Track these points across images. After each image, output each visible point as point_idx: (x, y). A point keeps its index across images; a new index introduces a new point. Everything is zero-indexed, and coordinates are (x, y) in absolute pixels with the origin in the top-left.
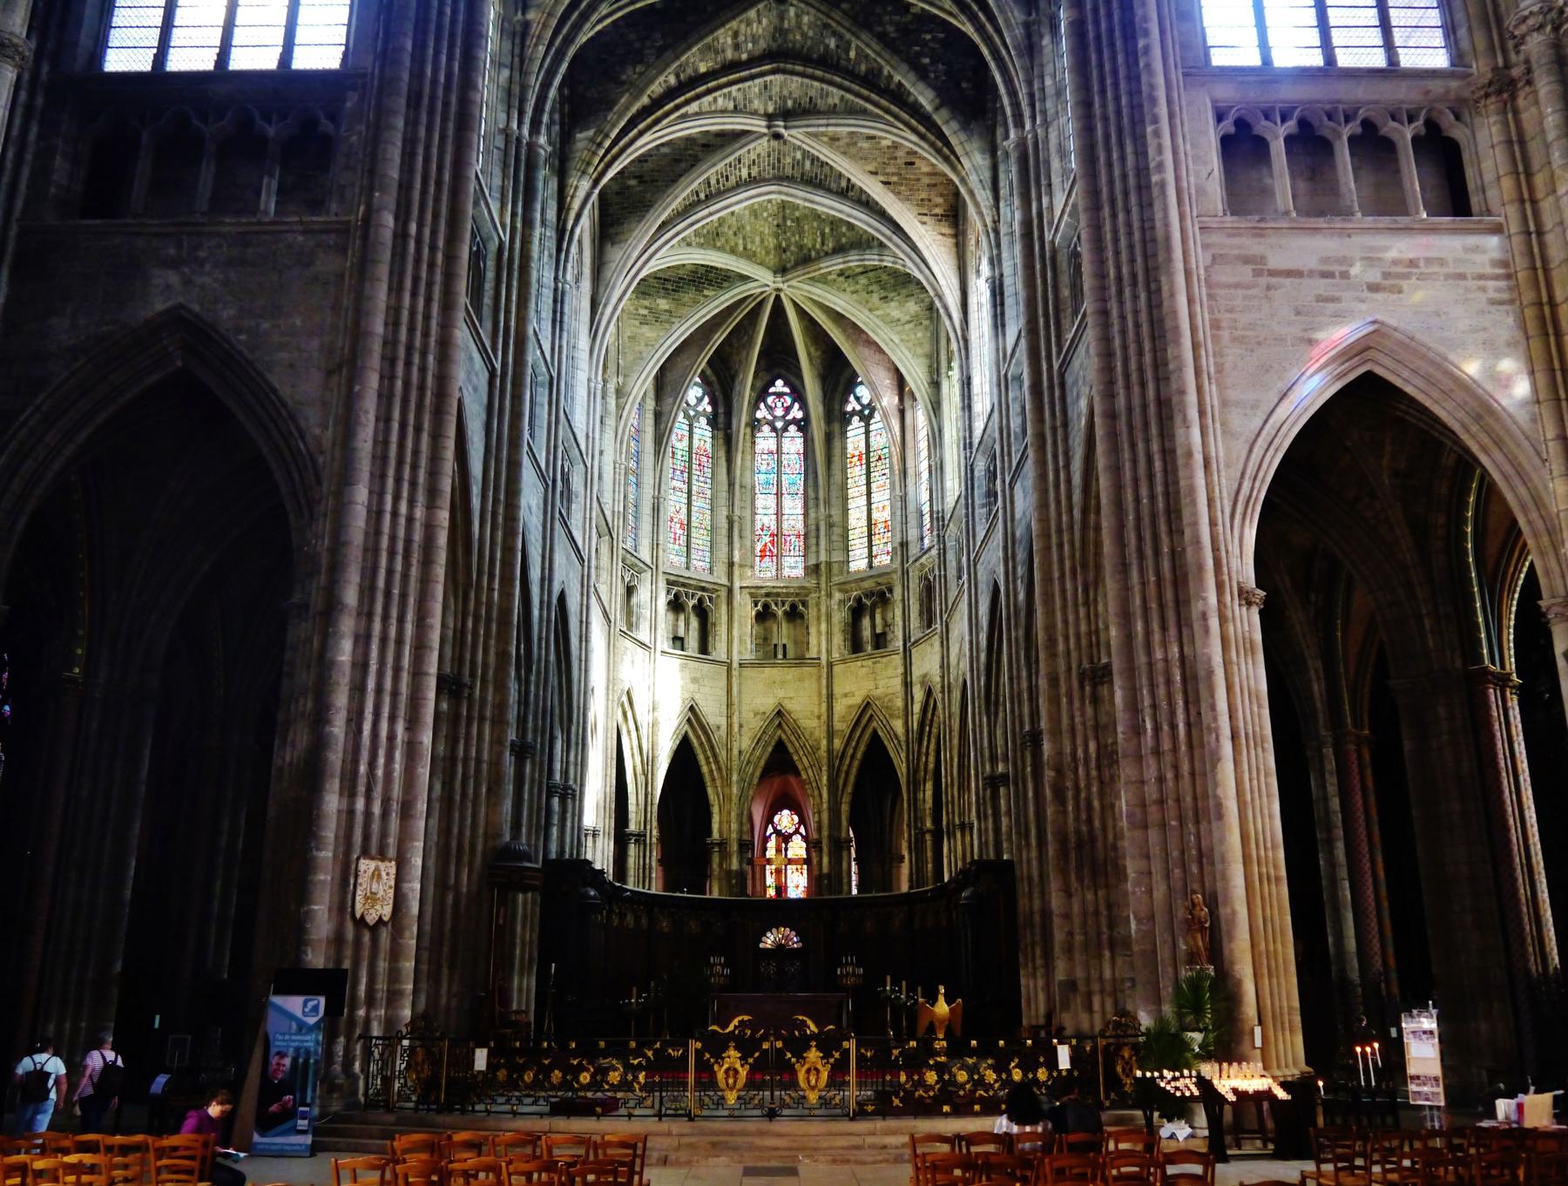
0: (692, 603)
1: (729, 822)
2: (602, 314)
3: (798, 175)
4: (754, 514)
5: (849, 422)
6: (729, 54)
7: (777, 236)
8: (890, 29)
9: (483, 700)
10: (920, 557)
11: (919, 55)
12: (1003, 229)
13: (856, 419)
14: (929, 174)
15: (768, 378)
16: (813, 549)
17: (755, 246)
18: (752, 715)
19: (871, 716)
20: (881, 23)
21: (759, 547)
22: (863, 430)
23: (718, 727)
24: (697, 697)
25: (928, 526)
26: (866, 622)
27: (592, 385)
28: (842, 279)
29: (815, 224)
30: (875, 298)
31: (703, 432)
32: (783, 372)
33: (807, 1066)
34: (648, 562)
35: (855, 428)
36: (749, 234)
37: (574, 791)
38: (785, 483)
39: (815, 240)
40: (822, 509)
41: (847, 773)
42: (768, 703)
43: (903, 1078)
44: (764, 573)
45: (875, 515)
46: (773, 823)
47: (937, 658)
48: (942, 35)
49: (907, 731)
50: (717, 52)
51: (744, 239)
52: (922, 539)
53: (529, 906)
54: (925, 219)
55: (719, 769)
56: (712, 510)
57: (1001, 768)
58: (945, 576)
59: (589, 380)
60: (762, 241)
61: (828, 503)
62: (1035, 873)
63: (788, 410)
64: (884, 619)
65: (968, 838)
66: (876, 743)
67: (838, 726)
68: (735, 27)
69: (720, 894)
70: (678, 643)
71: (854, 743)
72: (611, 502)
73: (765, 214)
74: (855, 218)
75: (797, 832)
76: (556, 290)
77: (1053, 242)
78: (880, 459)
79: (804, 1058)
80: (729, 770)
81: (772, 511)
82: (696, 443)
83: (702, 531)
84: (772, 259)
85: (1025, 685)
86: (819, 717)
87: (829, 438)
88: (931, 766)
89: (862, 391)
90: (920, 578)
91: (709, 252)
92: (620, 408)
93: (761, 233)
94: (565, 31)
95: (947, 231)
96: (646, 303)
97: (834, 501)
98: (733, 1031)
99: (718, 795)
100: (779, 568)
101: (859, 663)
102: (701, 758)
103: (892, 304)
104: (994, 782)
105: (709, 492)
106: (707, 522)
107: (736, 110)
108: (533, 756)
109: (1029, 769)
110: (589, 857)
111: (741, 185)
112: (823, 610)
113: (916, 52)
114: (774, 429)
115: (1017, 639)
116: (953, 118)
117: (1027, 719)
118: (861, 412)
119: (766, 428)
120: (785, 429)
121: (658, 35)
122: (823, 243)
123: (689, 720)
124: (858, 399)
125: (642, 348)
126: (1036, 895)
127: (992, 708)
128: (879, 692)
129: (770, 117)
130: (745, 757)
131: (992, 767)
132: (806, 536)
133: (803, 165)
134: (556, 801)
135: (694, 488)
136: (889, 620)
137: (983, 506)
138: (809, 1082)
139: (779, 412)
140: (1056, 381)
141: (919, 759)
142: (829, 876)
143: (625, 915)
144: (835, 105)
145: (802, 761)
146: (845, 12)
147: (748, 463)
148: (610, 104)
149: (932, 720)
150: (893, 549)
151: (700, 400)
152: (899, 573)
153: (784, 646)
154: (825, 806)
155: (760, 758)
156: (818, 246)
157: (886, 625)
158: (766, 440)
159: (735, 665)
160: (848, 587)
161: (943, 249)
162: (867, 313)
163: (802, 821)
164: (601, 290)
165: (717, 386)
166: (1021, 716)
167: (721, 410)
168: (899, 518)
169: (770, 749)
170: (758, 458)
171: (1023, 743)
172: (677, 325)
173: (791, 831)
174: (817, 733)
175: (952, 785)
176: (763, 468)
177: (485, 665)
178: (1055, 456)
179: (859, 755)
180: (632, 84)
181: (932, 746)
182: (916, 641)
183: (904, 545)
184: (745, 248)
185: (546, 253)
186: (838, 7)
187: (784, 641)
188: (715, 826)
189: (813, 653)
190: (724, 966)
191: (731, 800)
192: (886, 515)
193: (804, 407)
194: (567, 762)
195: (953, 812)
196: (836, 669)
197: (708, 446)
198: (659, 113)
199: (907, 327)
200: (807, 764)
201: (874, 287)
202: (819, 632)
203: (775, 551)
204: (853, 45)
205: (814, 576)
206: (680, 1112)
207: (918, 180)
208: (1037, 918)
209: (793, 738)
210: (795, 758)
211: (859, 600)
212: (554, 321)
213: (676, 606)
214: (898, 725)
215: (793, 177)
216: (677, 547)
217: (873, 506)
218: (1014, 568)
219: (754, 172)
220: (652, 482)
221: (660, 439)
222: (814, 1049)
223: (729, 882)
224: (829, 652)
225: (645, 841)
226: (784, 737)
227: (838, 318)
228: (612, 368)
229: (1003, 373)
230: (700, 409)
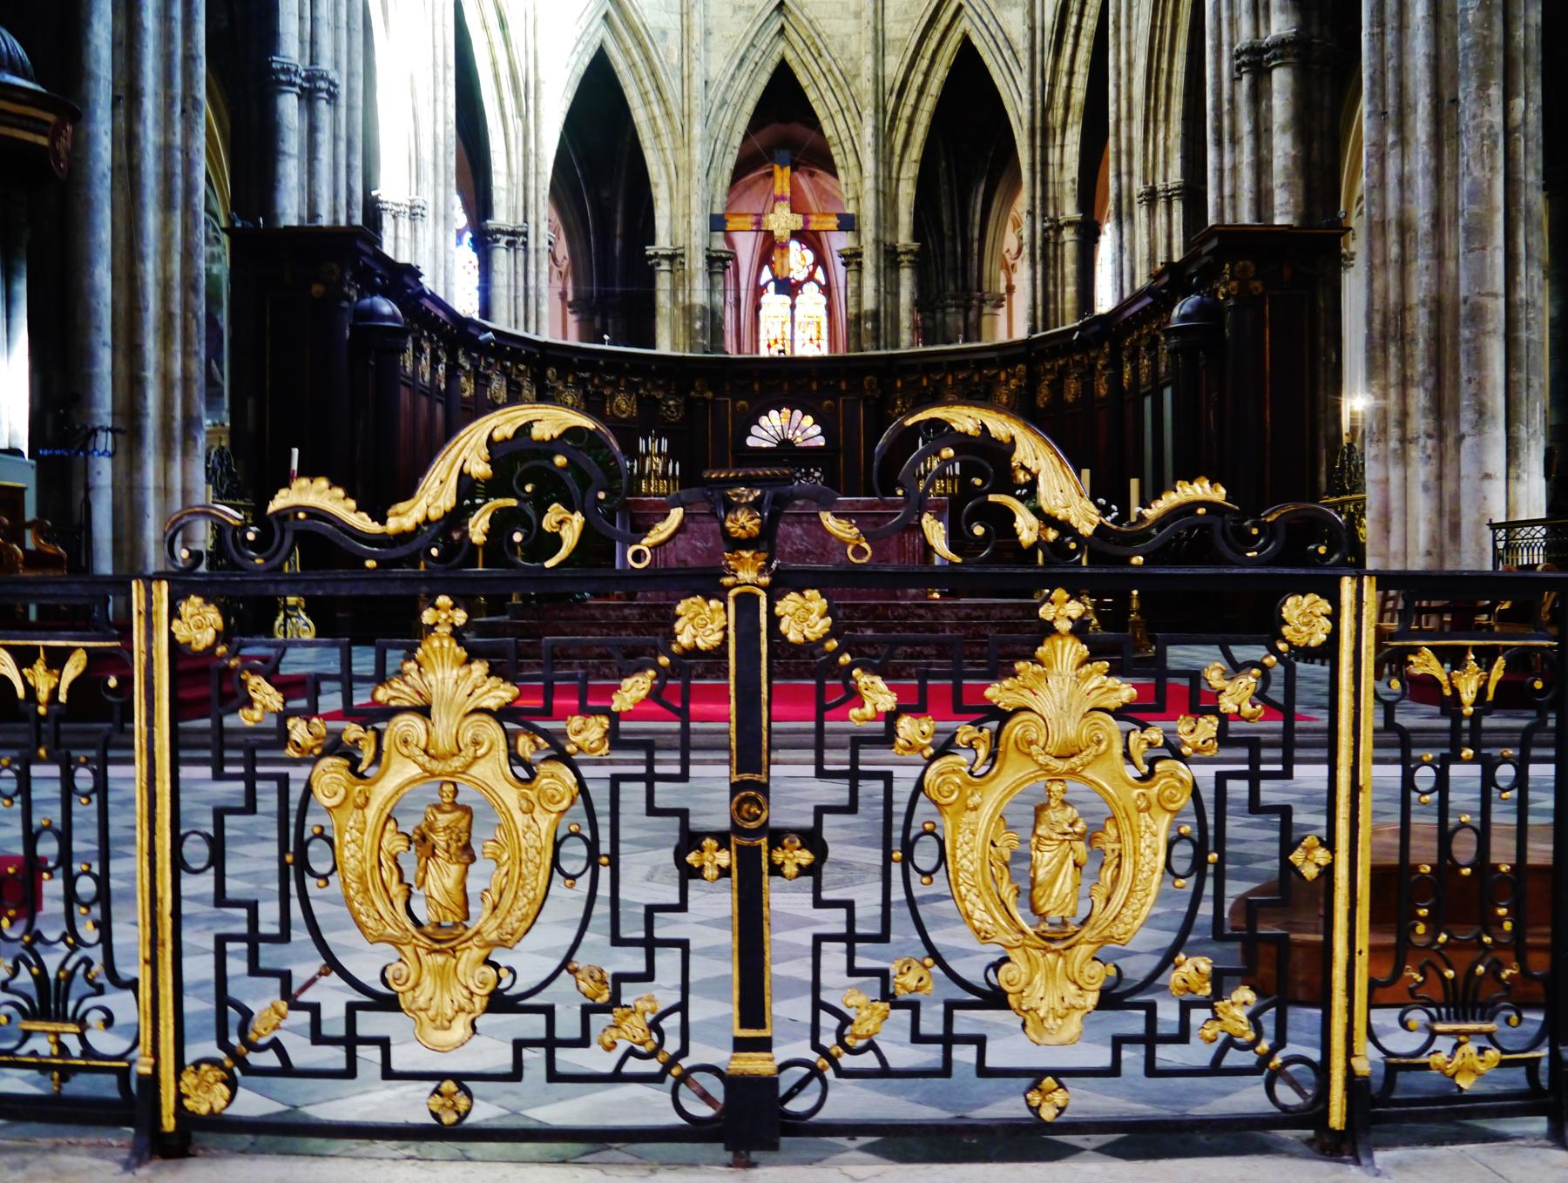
18: (728, 11)
19: (960, 7)
23: (664, 33)
33: (1014, 773)
37: (332, 83)
41: (911, 123)
49: (1032, 29)
53: (177, 296)
55: (668, 114)
65: (1161, 219)
66: (968, 62)
69: (674, 345)
71: (924, 64)
75: (811, 277)
80: (687, 116)
86: (858, 15)
88: (1079, 96)
98: (458, 516)
99: (666, 165)
110: (404, 258)
123: (606, 17)
126: (1421, 262)
130: (715, 94)
134: (289, 106)
138: (1029, 894)
141: (1053, 85)
142: (875, 315)
143: (488, 379)
154: (869, 183)
155: (744, 96)
163: (820, 260)
169: (764, 79)
174: (853, 46)
175: (1130, 117)
179: (935, 87)
181: (1083, 55)
190: (667, 457)
191: (690, 172)
194: (313, 19)
195: (1130, 173)
200: (834, 108)
206: (80, 1086)
208: (1420, 320)
209: (808, 58)
210: (812, 95)
214: (1014, 22)
222: (1066, 652)
223: (689, 328)
225: (525, 244)
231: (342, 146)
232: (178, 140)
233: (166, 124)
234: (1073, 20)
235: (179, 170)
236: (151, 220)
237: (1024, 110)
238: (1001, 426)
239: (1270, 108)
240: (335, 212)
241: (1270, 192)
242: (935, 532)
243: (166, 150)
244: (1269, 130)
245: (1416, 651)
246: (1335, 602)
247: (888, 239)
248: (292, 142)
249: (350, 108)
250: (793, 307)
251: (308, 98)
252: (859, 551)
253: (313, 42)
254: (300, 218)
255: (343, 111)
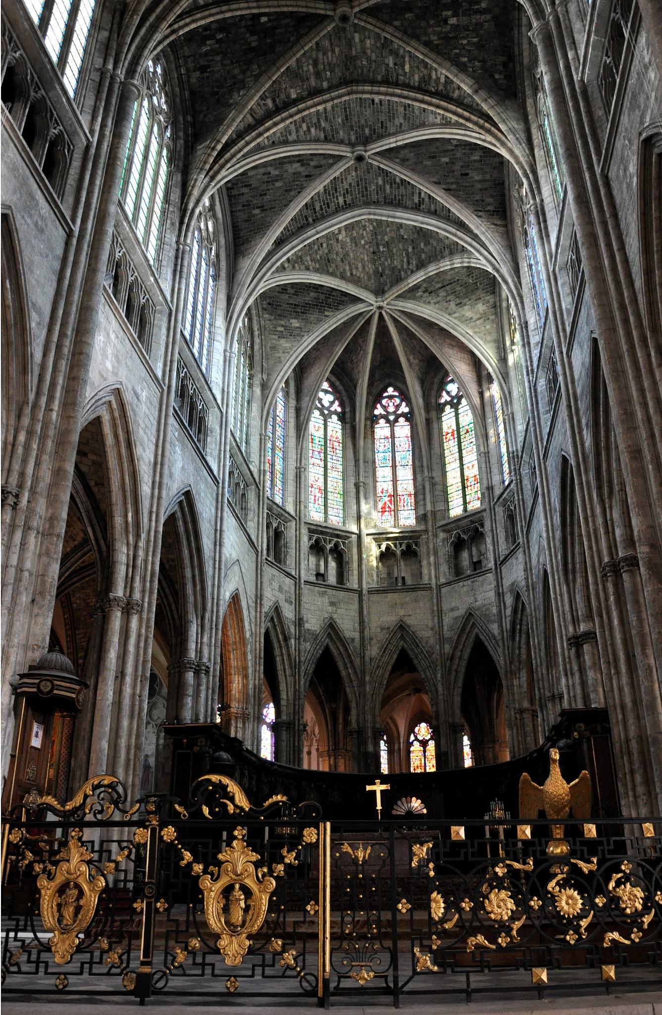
0: (329, 547)
1: (364, 714)
2: (236, 304)
3: (381, 199)
4: (375, 481)
5: (443, 410)
6: (313, 82)
7: (373, 261)
8: (434, 38)
9: (30, 511)
10: (503, 493)
11: (458, 56)
12: (540, 165)
13: (448, 408)
14: (480, 181)
15: (382, 386)
16: (422, 503)
17: (358, 273)
20: (426, 34)
21: (380, 505)
22: (453, 414)
23: (353, 640)
24: (335, 616)
25: (508, 471)
26: (465, 555)
27: (228, 354)
28: (427, 294)
29: (401, 246)
30: (452, 305)
31: (335, 427)
32: (392, 381)
34: (293, 513)
35: (448, 414)
36: (353, 261)
37: (207, 667)
38: (398, 459)
39: (402, 261)
40: (426, 473)
42: (390, 620)
43: (438, 907)
44: (387, 524)
45: (467, 473)
46: (414, 733)
47: (521, 567)
48: (475, 40)
49: (502, 631)
50: (303, 81)
51: (350, 266)
52: (504, 482)
53: (133, 751)
54: (480, 214)
55: (356, 673)
56: (343, 480)
57: (583, 627)
58: (523, 500)
59: (225, 351)
60: (364, 268)
61: (430, 469)
62: (628, 700)
63: (397, 407)
64: (479, 551)
67: (447, 633)
68: (314, 56)
70: (319, 578)
72: (257, 463)
73: (363, 242)
74: (427, 224)
76: (177, 250)
77: (582, 80)
78: (467, 432)
79: (219, 864)
80: (363, 673)
81: (389, 477)
82: (329, 433)
83: (336, 495)
84: (372, 283)
85: (600, 520)
86: (432, 629)
87: (428, 422)
88: (524, 657)
89: (453, 388)
90: (504, 512)
91: (323, 276)
92: (264, 398)
93: (363, 259)
94: (158, 10)
95: (499, 223)
96: (282, 322)
97: (435, 467)
100: (396, 518)
101: (461, 584)
102: (340, 665)
103: (465, 307)
104: (577, 642)
105: (340, 468)
106: (340, 489)
107: (327, 140)
108: (141, 612)
109: (612, 598)
110: (240, 736)
111: (338, 210)
112: (431, 547)
113: (456, 54)
114: (388, 421)
115: (588, 483)
116: (490, 97)
117: (605, 552)
118: (452, 401)
119: (382, 421)
120: (396, 420)
121: (255, 67)
122: (408, 263)
123: (329, 633)
124: (448, 393)
125: (280, 355)
127: (571, 577)
128: (479, 603)
129: (352, 145)
131: (575, 628)
132: (416, 495)
133: (385, 190)
134: (190, 676)
135: (329, 465)
136: (483, 551)
137: (548, 412)
139: (391, 409)
140: (600, 183)
141: (513, 653)
144: (401, 124)
145: (421, 663)
146: (396, 27)
147: (370, 446)
148: (220, 121)
149: (521, 620)
150: (483, 494)
151: (332, 403)
152: (488, 511)
153: (403, 578)
156: (405, 267)
157: (481, 554)
158: (382, 430)
159: (364, 592)
160: (449, 527)
161: (497, 234)
162: (448, 316)
164: (235, 288)
165: (344, 393)
166: (599, 552)
167: (348, 410)
168: (484, 469)
169: (395, 656)
170: (377, 442)
171: (605, 575)
172: (306, 337)
173: (427, 738)
174: (432, 641)
175: (541, 665)
176: (381, 449)
177: (36, 479)
178: (609, 245)
179: (466, 656)
180: (237, 104)
181: (523, 641)
182: (502, 562)
183: (490, 488)
184: (352, 274)
185: (169, 222)
186: (391, 24)
187: (403, 575)
188: (353, 718)
189: (426, 580)
192: (475, 471)
193: (409, 404)
194: (201, 643)
195: (544, 688)
196: (443, 590)
197: (339, 435)
198: (262, 129)
199: (478, 322)
201: (451, 297)
202: (429, 564)
203: (392, 507)
204: (407, 59)
205: (423, 522)
207: (472, 186)
211: (459, 537)
212: (175, 271)
213: (317, 548)
215: (378, 202)
216: (316, 506)
217: (465, 467)
218: (579, 421)
219: (349, 199)
220: (294, 457)
221: (301, 427)
224: (437, 578)
226: (406, 646)
227: (428, 325)
228: (257, 367)
229: (551, 270)
230: (332, 409)
231: (210, 691)
232: (138, 692)
233: (134, 687)
234: (518, 627)
235: (137, 703)
236: (125, 723)
237: (502, 662)
238: (226, 780)
239: (584, 660)
240: (206, 717)
241: (589, 694)
242: (206, 810)
243: (133, 695)
244: (585, 669)
245: (343, 844)
246: (318, 830)
247: (450, 720)
248: (190, 691)
249: (214, 676)
250: (425, 751)
251: (197, 673)
252: (184, 816)
253: (201, 652)
254: (191, 720)
255: (211, 678)
